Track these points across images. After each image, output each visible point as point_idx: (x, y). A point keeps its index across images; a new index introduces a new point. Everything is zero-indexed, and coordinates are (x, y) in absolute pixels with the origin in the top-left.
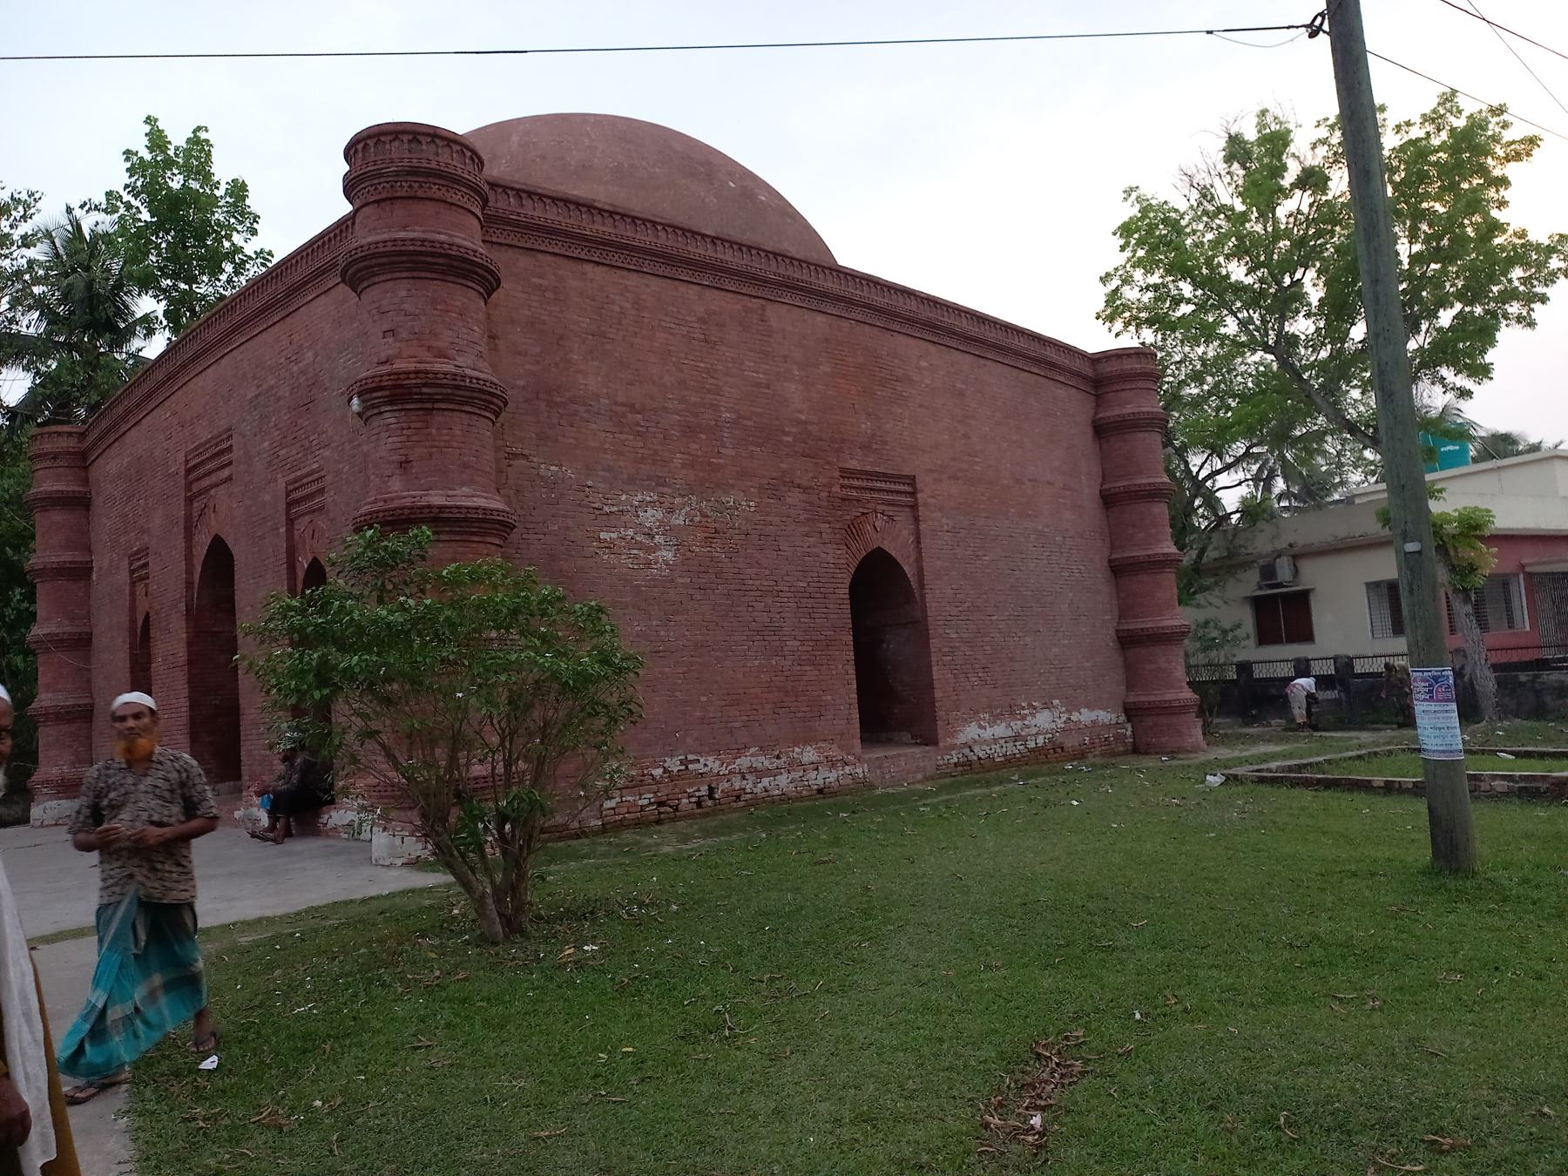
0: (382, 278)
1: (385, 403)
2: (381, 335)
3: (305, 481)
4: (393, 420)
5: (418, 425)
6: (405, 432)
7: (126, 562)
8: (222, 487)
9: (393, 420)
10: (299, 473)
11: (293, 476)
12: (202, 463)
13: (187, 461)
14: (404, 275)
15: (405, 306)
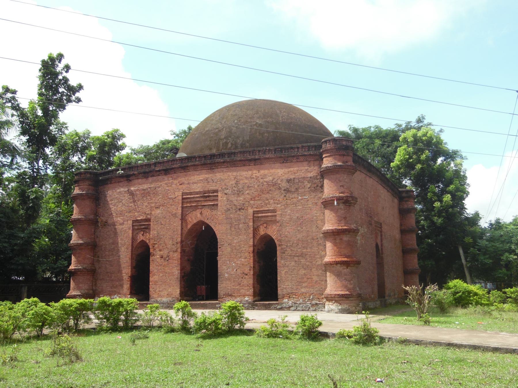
0: (341, 173)
1: (341, 203)
2: (339, 186)
3: (263, 212)
4: (342, 207)
5: (348, 209)
6: (345, 210)
7: (130, 222)
8: (207, 206)
9: (342, 207)
10: (262, 209)
11: (258, 210)
12: (194, 198)
13: (182, 196)
14: (346, 173)
15: (346, 180)
